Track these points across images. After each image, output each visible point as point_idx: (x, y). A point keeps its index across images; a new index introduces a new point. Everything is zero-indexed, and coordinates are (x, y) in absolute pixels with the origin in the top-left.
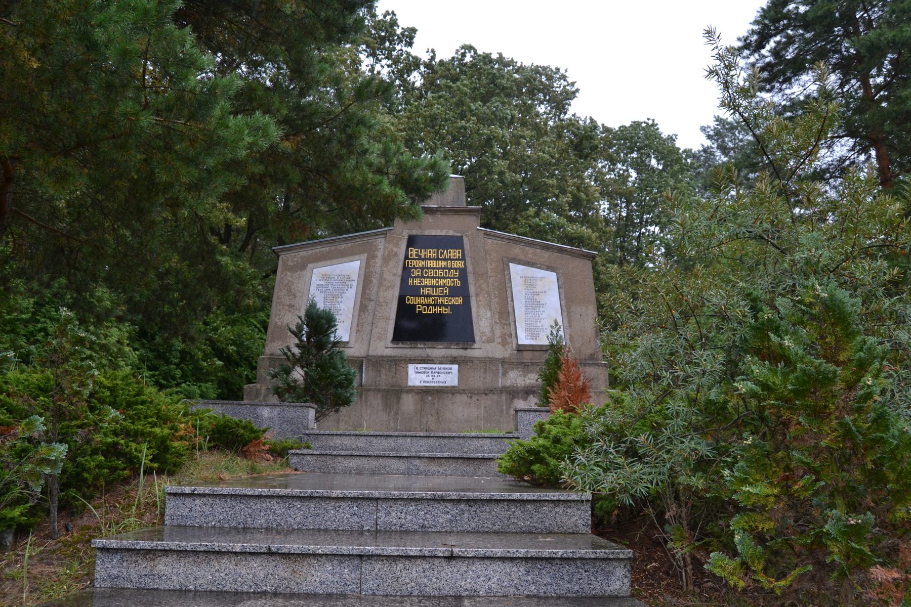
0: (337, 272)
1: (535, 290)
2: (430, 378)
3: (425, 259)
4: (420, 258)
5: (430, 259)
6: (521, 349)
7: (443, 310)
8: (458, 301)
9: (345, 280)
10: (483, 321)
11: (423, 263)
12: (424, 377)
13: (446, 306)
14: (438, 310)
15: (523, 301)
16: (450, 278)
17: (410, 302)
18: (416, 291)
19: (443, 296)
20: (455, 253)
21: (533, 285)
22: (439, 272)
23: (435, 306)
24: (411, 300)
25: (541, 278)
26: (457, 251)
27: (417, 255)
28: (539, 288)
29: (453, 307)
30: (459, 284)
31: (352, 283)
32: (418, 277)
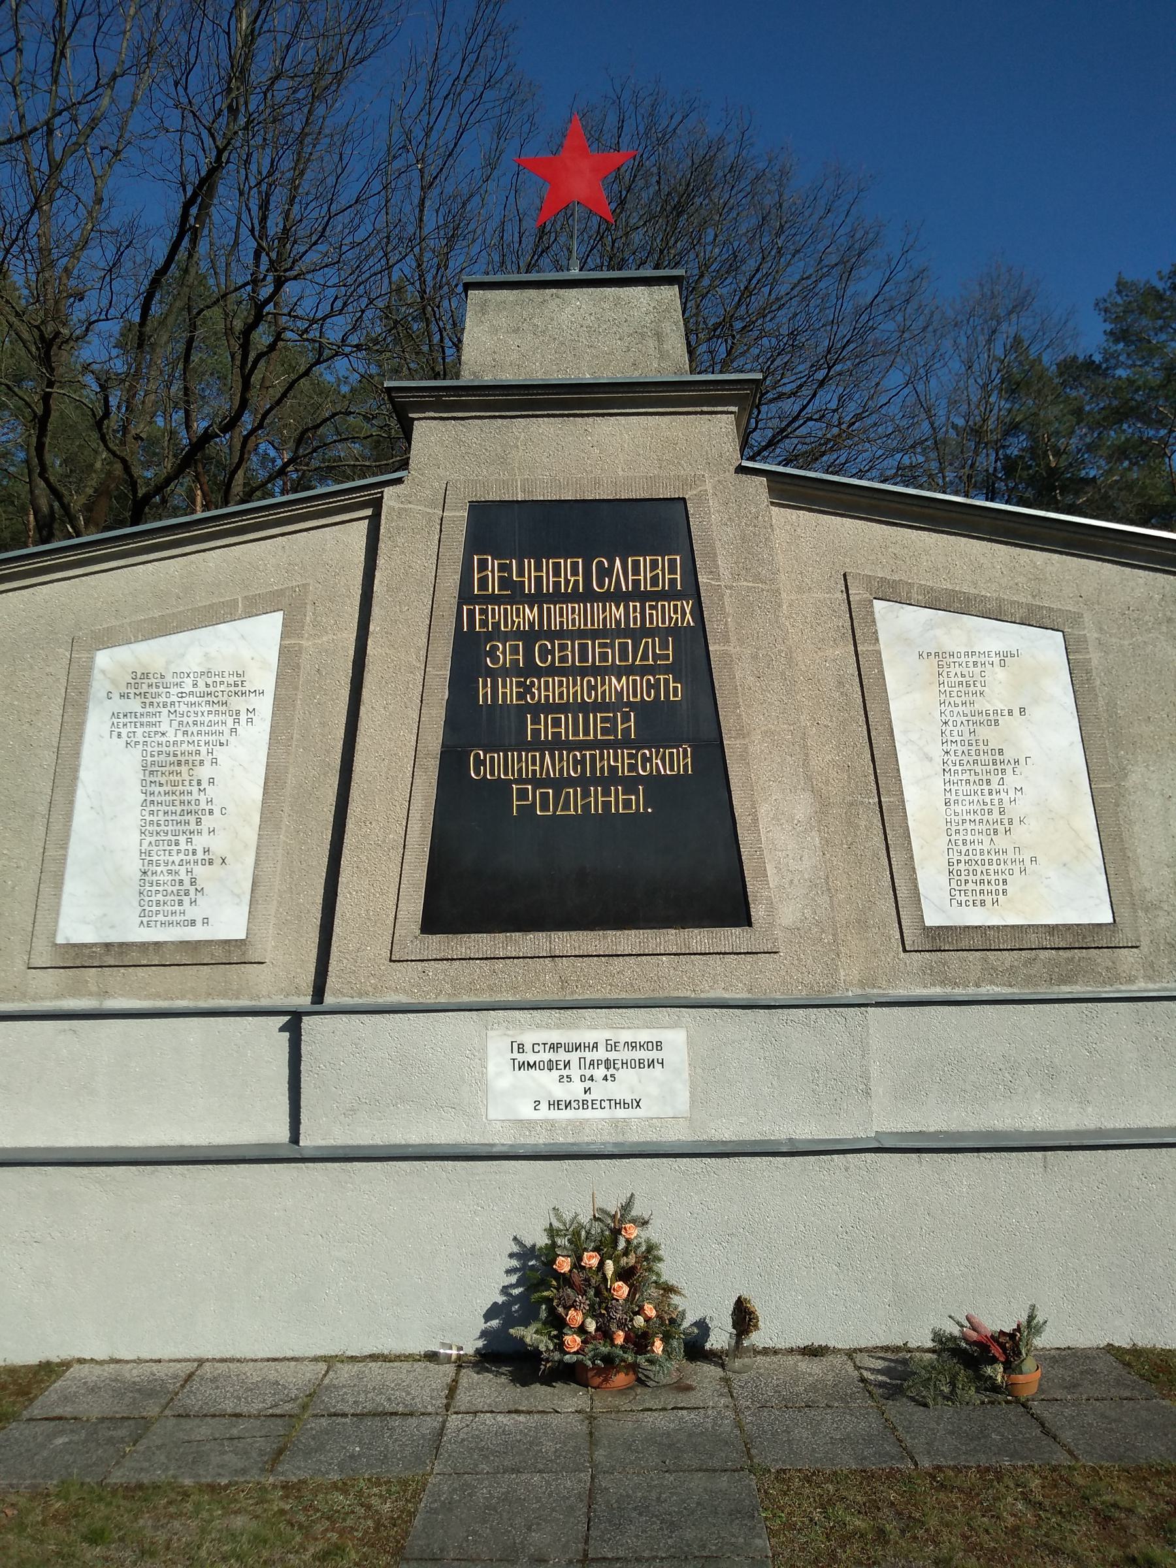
0: (193, 662)
1: (981, 704)
2: (575, 1090)
3: (537, 599)
5: (558, 597)
8: (673, 762)
9: (223, 692)
10: (781, 835)
11: (531, 614)
13: (630, 785)
14: (597, 799)
15: (937, 752)
16: (644, 671)
19: (614, 745)
20: (652, 570)
21: (971, 687)
22: (594, 650)
23: (583, 782)
24: (491, 766)
25: (1004, 658)
26: (663, 561)
27: (505, 583)
28: (997, 696)
29: (655, 783)
30: (675, 690)
31: (254, 701)
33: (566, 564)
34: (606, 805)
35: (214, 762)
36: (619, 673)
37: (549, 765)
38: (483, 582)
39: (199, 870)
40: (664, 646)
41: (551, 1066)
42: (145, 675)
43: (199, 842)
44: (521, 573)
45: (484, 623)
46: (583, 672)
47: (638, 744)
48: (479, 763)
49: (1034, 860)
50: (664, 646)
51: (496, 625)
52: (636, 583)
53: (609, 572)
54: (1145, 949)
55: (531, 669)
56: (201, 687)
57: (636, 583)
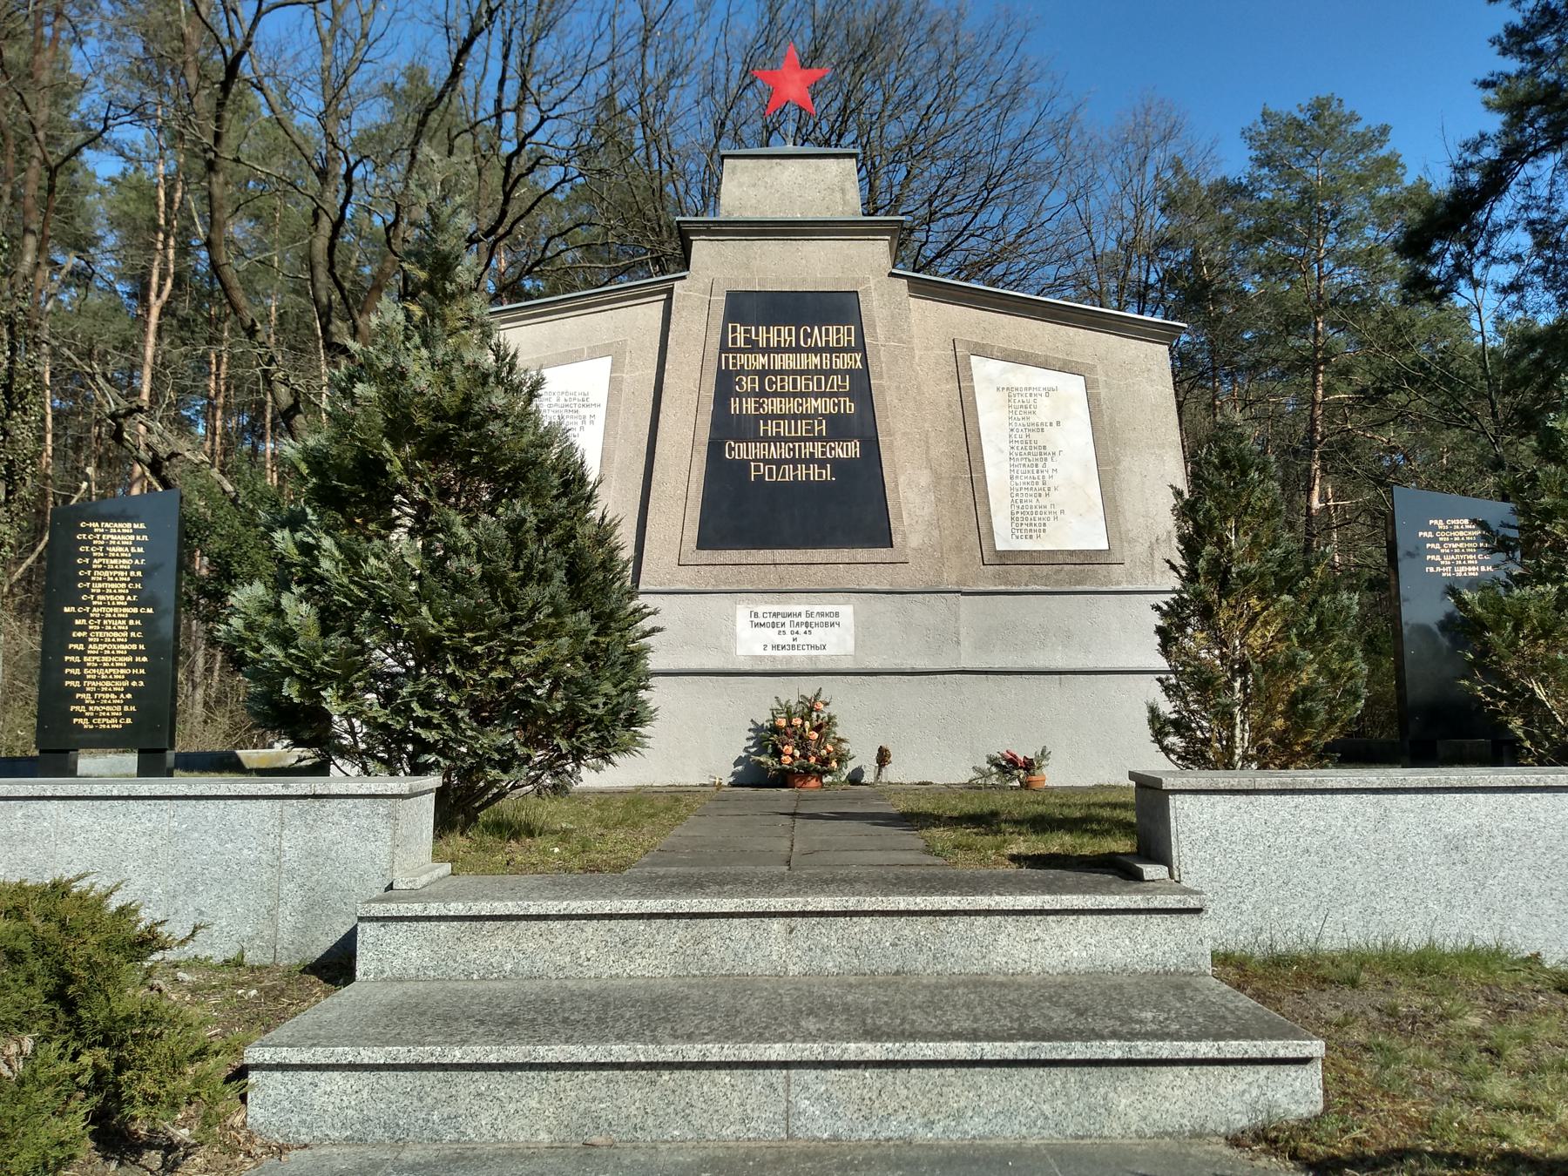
1: (1033, 419)
3: (767, 350)
4: (752, 347)
5: (779, 350)
7: (814, 472)
8: (849, 450)
10: (911, 493)
11: (762, 360)
12: (772, 635)
13: (822, 464)
15: (1006, 448)
16: (831, 395)
17: (735, 455)
18: (745, 429)
21: (1030, 409)
22: (801, 382)
23: (794, 462)
24: (739, 451)
25: (1048, 391)
27: (747, 341)
29: (837, 464)
30: (850, 407)
32: (753, 394)
33: (785, 330)
34: (808, 475)
36: (817, 396)
37: (774, 452)
38: (734, 340)
40: (844, 380)
41: (774, 625)
45: (735, 365)
46: (795, 395)
48: (731, 449)
49: (1062, 512)
50: (844, 380)
52: (827, 342)
53: (810, 335)
55: (762, 393)
57: (827, 342)
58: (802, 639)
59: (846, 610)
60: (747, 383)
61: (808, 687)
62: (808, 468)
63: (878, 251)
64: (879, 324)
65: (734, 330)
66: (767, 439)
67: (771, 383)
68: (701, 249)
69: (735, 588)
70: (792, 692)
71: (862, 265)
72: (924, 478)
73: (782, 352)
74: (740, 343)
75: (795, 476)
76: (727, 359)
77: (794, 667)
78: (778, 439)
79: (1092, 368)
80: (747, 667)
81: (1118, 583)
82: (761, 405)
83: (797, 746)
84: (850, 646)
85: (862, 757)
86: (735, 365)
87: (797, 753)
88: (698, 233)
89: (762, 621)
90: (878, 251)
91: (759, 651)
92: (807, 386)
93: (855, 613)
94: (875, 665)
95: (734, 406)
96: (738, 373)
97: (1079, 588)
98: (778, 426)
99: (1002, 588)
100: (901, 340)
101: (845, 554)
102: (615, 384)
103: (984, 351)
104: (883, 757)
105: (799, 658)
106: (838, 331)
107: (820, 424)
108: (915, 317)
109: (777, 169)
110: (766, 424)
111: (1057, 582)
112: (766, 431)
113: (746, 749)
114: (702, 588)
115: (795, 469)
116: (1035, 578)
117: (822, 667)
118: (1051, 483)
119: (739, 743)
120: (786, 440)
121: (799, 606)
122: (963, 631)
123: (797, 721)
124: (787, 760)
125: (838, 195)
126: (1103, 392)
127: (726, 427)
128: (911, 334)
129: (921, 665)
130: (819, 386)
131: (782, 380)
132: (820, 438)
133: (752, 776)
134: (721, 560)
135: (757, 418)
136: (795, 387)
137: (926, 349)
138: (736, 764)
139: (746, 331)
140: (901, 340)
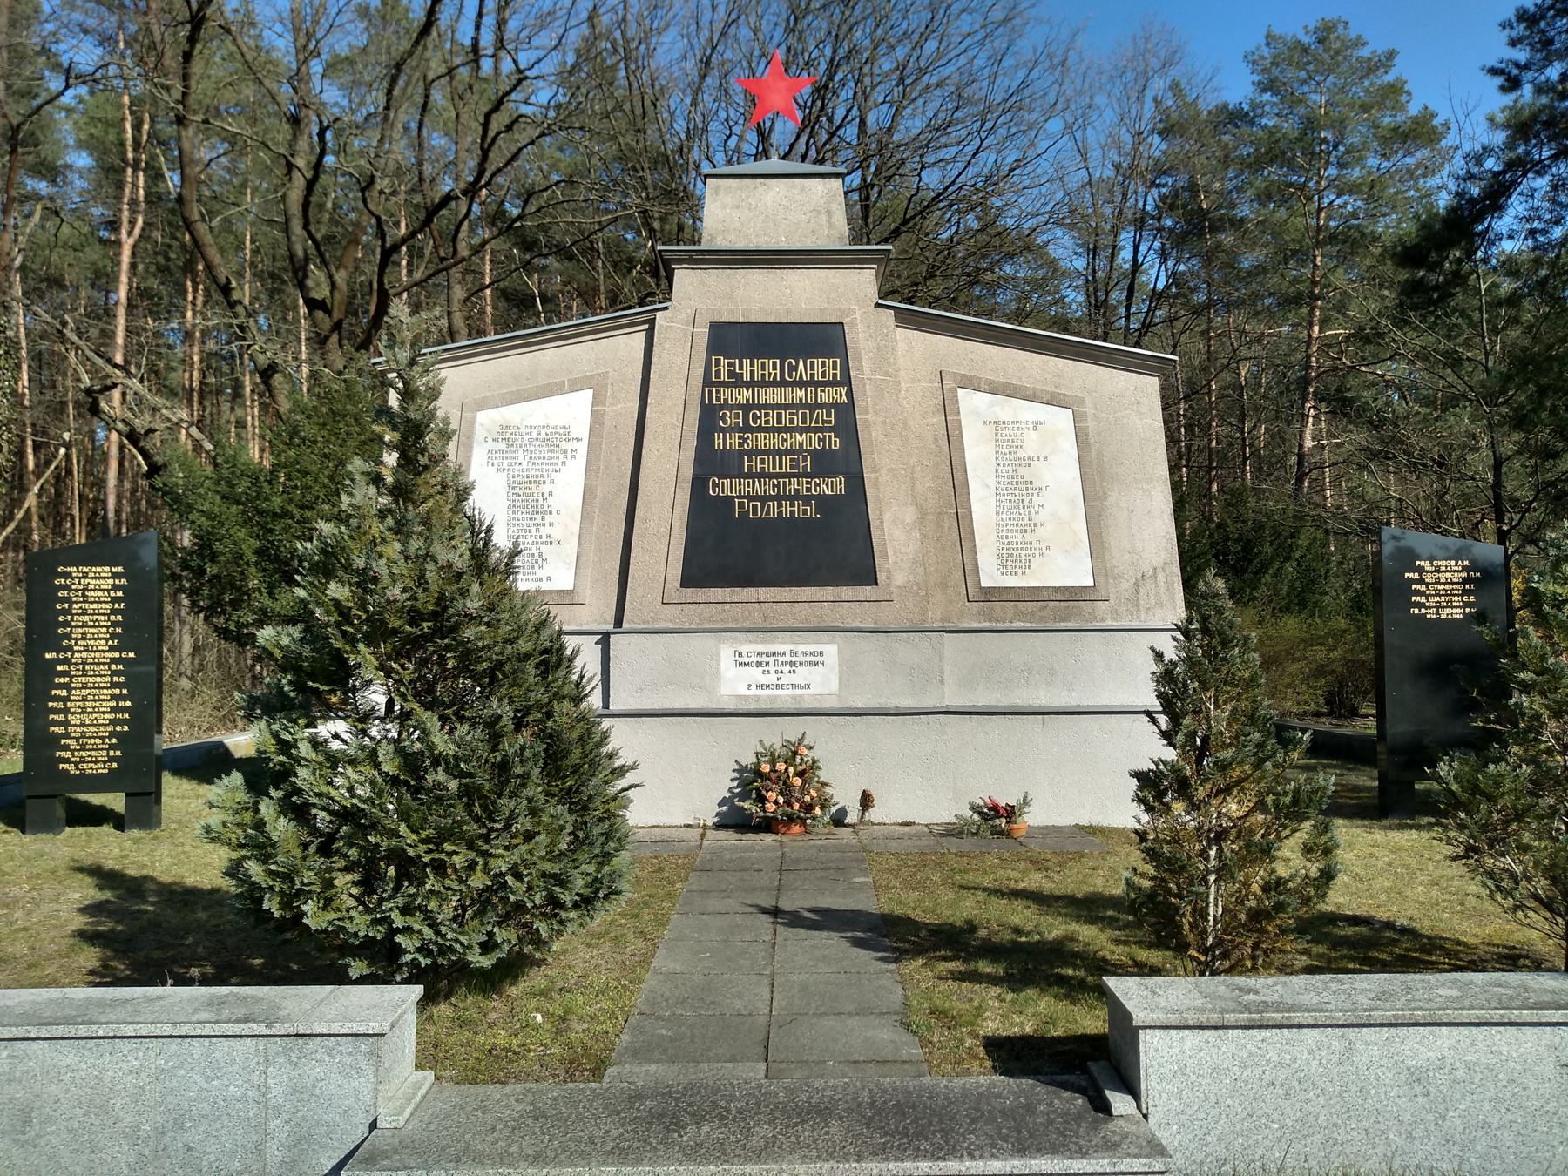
0: (538, 420)
2: (772, 678)
3: (751, 384)
4: (736, 381)
5: (764, 383)
6: (991, 595)
7: (799, 509)
8: (834, 486)
9: (557, 437)
11: (747, 394)
12: (756, 674)
13: (807, 500)
15: (992, 482)
16: (817, 430)
19: (797, 476)
21: (1015, 443)
22: (786, 417)
23: (779, 498)
24: (722, 487)
25: (1036, 425)
26: (829, 362)
27: (731, 374)
29: (822, 501)
30: (835, 442)
31: (575, 445)
33: (769, 363)
34: (792, 512)
35: (552, 482)
36: (802, 431)
37: (758, 488)
38: (718, 373)
39: (543, 548)
40: (829, 415)
41: (758, 664)
42: (508, 427)
43: (544, 531)
44: (741, 368)
45: (718, 399)
46: (779, 430)
47: (811, 476)
48: (715, 485)
50: (829, 415)
51: (726, 400)
52: (812, 375)
53: (795, 368)
54: (1112, 602)
55: (746, 428)
56: (543, 436)
57: (812, 375)
58: (785, 680)
59: (830, 649)
60: (731, 419)
61: (790, 730)
62: (792, 505)
63: (864, 281)
64: (865, 357)
65: (718, 363)
66: (751, 475)
67: (755, 418)
68: (684, 278)
69: (718, 626)
70: (776, 735)
71: (847, 296)
72: (910, 515)
73: (769, 386)
74: (724, 377)
75: (780, 513)
76: (710, 393)
77: (779, 706)
78: (762, 475)
79: (1081, 401)
80: (730, 706)
81: (1103, 620)
82: (745, 441)
83: (781, 793)
84: (834, 685)
85: (845, 796)
86: (718, 399)
87: (781, 800)
88: (680, 261)
89: (747, 660)
90: (864, 281)
91: (744, 691)
92: (792, 421)
93: (839, 652)
94: (860, 703)
95: (718, 441)
96: (722, 407)
97: (1063, 625)
98: (762, 462)
99: (987, 625)
100: (887, 374)
101: (829, 592)
102: (597, 418)
103: (970, 384)
104: (866, 801)
105: (784, 698)
106: (823, 364)
107: (805, 460)
108: (901, 347)
109: (761, 190)
110: (750, 460)
111: (1042, 619)
112: (750, 467)
113: (730, 790)
114: (686, 626)
115: (780, 506)
116: (1019, 615)
117: (806, 705)
118: (1037, 519)
119: (723, 784)
120: (771, 476)
121: (783, 645)
122: (947, 669)
123: (781, 766)
124: (770, 807)
125: (824, 217)
126: (1091, 425)
127: (710, 462)
128: (898, 364)
129: (905, 703)
130: (804, 421)
131: (767, 415)
132: (805, 474)
133: (734, 821)
134: (706, 598)
135: (742, 453)
136: (779, 422)
137: (913, 381)
138: (720, 805)
139: (730, 364)
140: (887, 374)
